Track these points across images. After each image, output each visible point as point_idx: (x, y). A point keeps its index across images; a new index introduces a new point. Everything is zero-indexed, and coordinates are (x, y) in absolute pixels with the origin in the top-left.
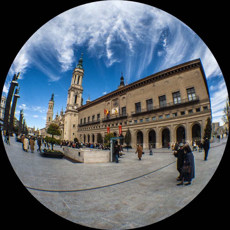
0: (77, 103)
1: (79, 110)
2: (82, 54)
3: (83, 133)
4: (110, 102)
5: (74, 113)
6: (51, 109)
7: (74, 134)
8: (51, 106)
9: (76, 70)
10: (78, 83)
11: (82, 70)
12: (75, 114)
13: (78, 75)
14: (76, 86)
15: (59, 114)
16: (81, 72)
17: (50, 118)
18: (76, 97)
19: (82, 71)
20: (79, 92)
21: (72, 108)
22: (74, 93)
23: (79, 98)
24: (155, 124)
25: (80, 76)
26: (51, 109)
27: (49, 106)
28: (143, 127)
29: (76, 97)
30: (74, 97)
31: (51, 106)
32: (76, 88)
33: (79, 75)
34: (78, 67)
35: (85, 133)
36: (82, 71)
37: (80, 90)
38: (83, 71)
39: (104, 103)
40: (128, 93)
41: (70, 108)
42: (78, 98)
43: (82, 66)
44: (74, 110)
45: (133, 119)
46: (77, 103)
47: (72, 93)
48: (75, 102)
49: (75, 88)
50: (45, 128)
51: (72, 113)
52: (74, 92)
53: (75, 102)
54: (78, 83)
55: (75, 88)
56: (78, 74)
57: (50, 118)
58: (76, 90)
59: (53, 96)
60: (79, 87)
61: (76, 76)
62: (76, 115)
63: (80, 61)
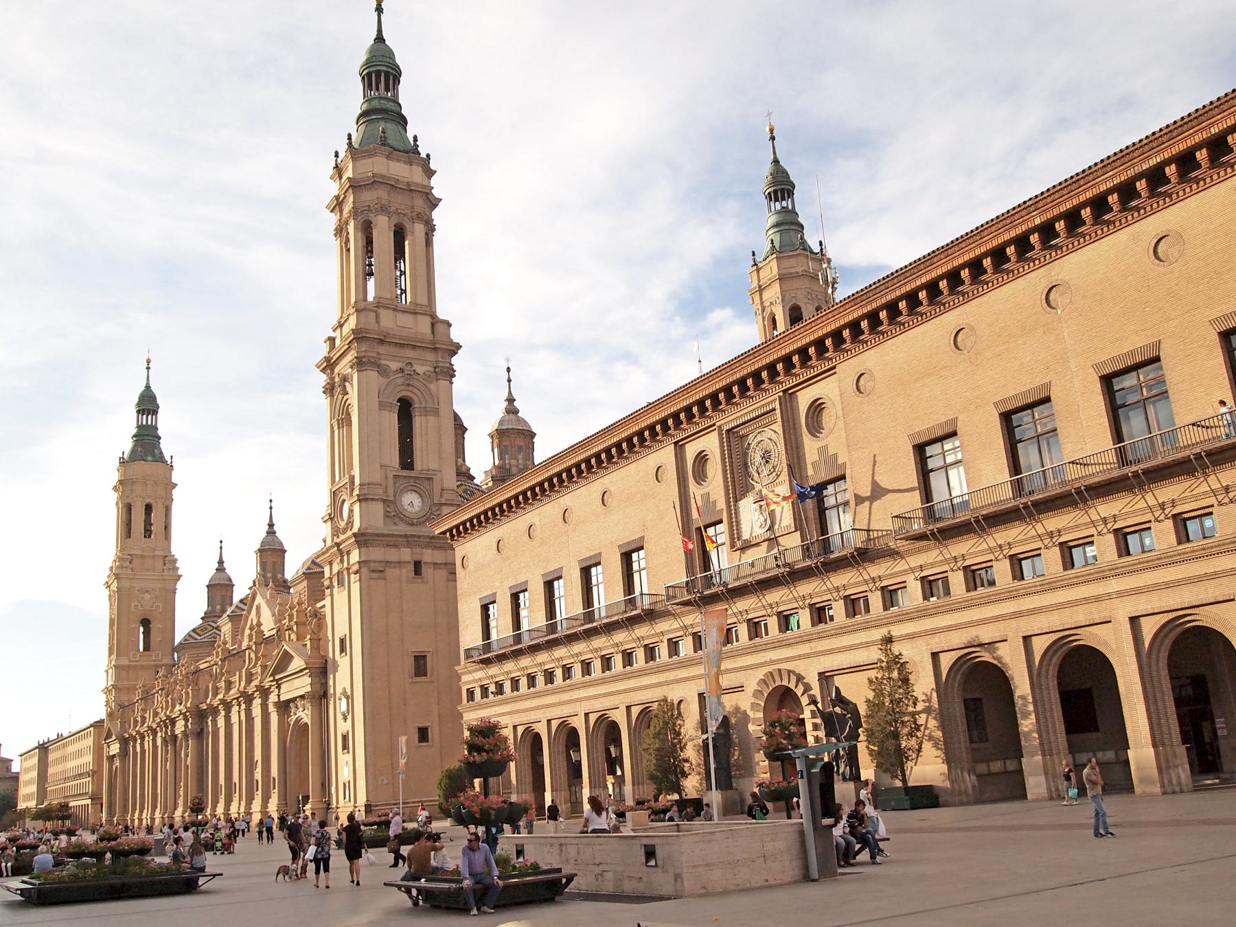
3: (517, 719)
5: (406, 554)
6: (148, 533)
7: (423, 734)
8: (148, 508)
12: (418, 567)
13: (389, 215)
15: (244, 575)
20: (421, 369)
21: (387, 515)
22: (383, 380)
24: (1097, 599)
25: (408, 225)
26: (148, 533)
28: (1002, 624)
30: (391, 420)
31: (148, 508)
33: (395, 220)
35: (532, 716)
39: (664, 455)
40: (848, 368)
42: (418, 422)
44: (403, 529)
45: (912, 570)
46: (418, 464)
50: (98, 725)
51: (392, 554)
52: (383, 371)
55: (382, 342)
56: (383, 209)
58: (395, 358)
62: (427, 571)
63: (378, 73)
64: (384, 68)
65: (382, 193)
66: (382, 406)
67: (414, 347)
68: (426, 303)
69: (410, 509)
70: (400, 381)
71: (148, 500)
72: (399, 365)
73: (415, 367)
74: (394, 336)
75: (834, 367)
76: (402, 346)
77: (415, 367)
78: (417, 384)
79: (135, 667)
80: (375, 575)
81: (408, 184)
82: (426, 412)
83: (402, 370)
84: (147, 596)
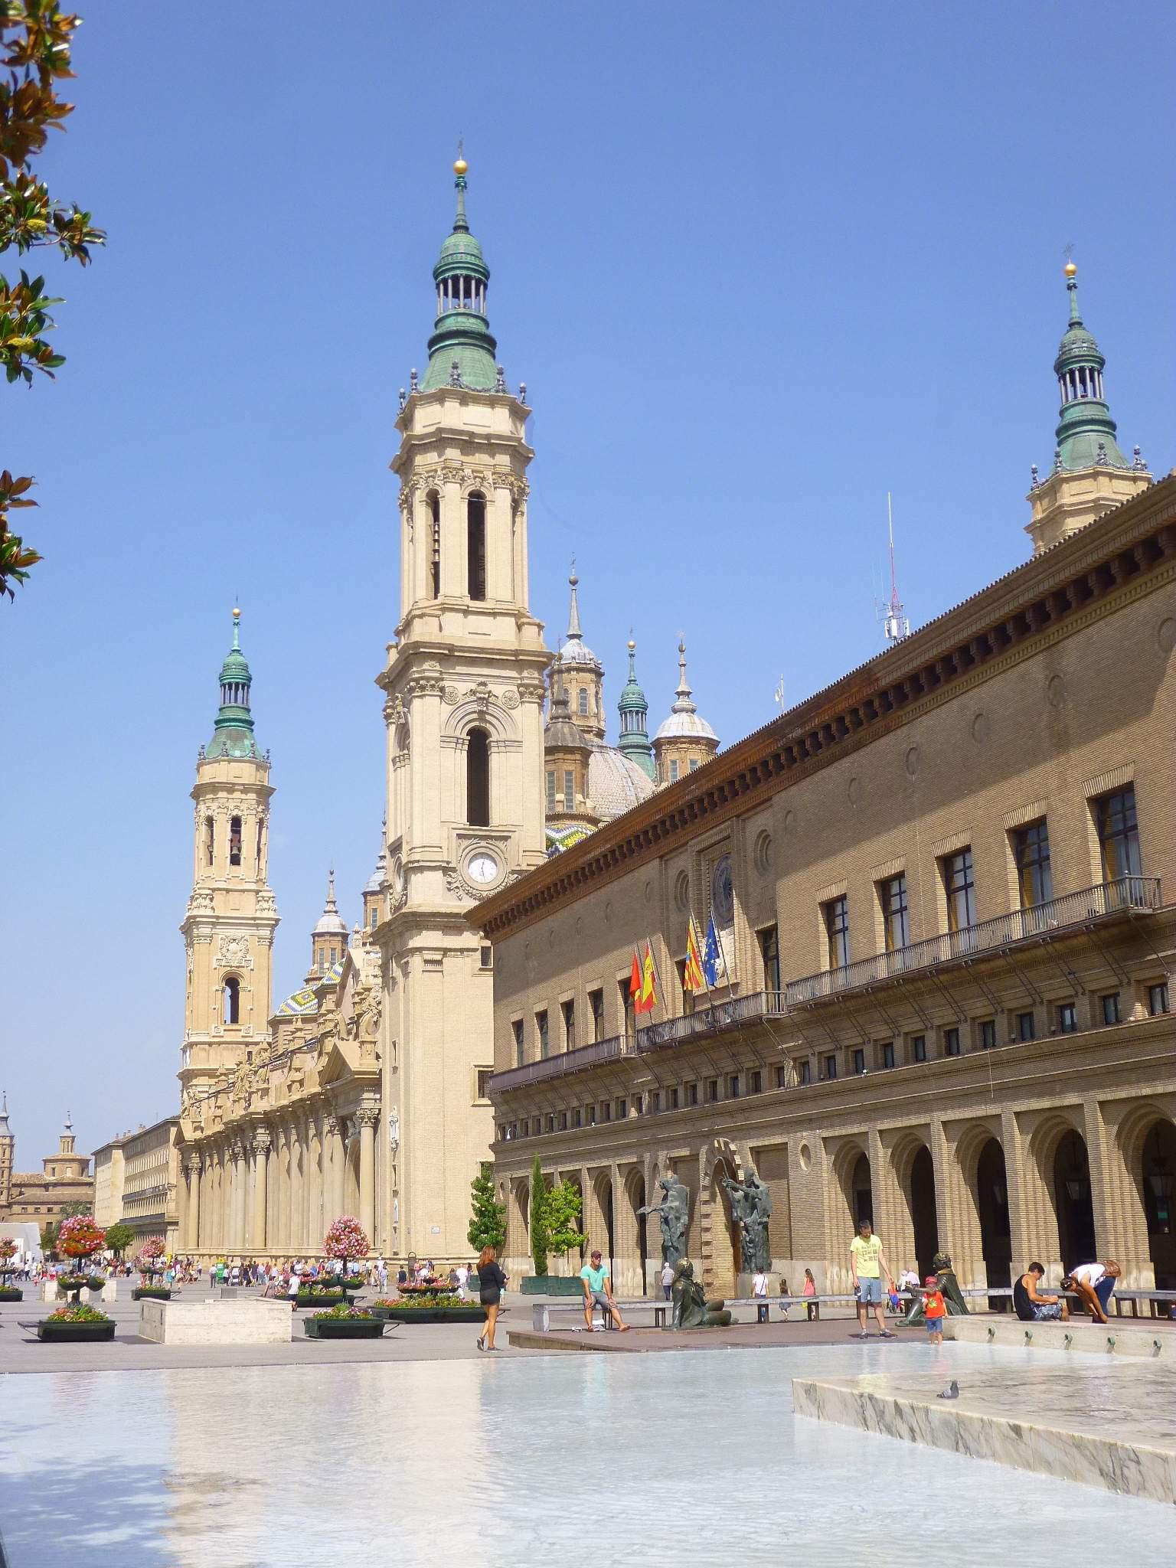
0: (500, 811)
1: (501, 918)
2: (461, 164)
4: (684, 861)
6: (235, 860)
8: (236, 823)
9: (425, 419)
10: (477, 589)
11: (492, 402)
14: (458, 630)
16: (490, 445)
17: (232, 982)
18: (478, 747)
19: (496, 421)
20: (498, 690)
22: (447, 709)
26: (235, 860)
27: (210, 821)
29: (478, 747)
30: (459, 762)
31: (236, 823)
32: (452, 648)
34: (436, 373)
36: (496, 421)
37: (516, 660)
38: (519, 413)
39: (649, 870)
41: (428, 893)
42: (497, 762)
43: (487, 343)
47: (430, 717)
48: (478, 808)
49: (449, 656)
53: (478, 808)
54: (477, 589)
56: (452, 473)
59: (237, 685)
60: (500, 634)
61: (434, 502)
64: (464, 272)
65: (453, 453)
66: (445, 739)
67: (490, 663)
68: (509, 598)
69: (479, 879)
70: (475, 707)
71: (234, 813)
72: (473, 686)
73: (490, 687)
74: (462, 649)
75: (769, 799)
76: (473, 662)
77: (490, 687)
78: (491, 709)
79: (219, 1044)
80: (430, 967)
81: (488, 437)
83: (473, 692)
84: (233, 946)
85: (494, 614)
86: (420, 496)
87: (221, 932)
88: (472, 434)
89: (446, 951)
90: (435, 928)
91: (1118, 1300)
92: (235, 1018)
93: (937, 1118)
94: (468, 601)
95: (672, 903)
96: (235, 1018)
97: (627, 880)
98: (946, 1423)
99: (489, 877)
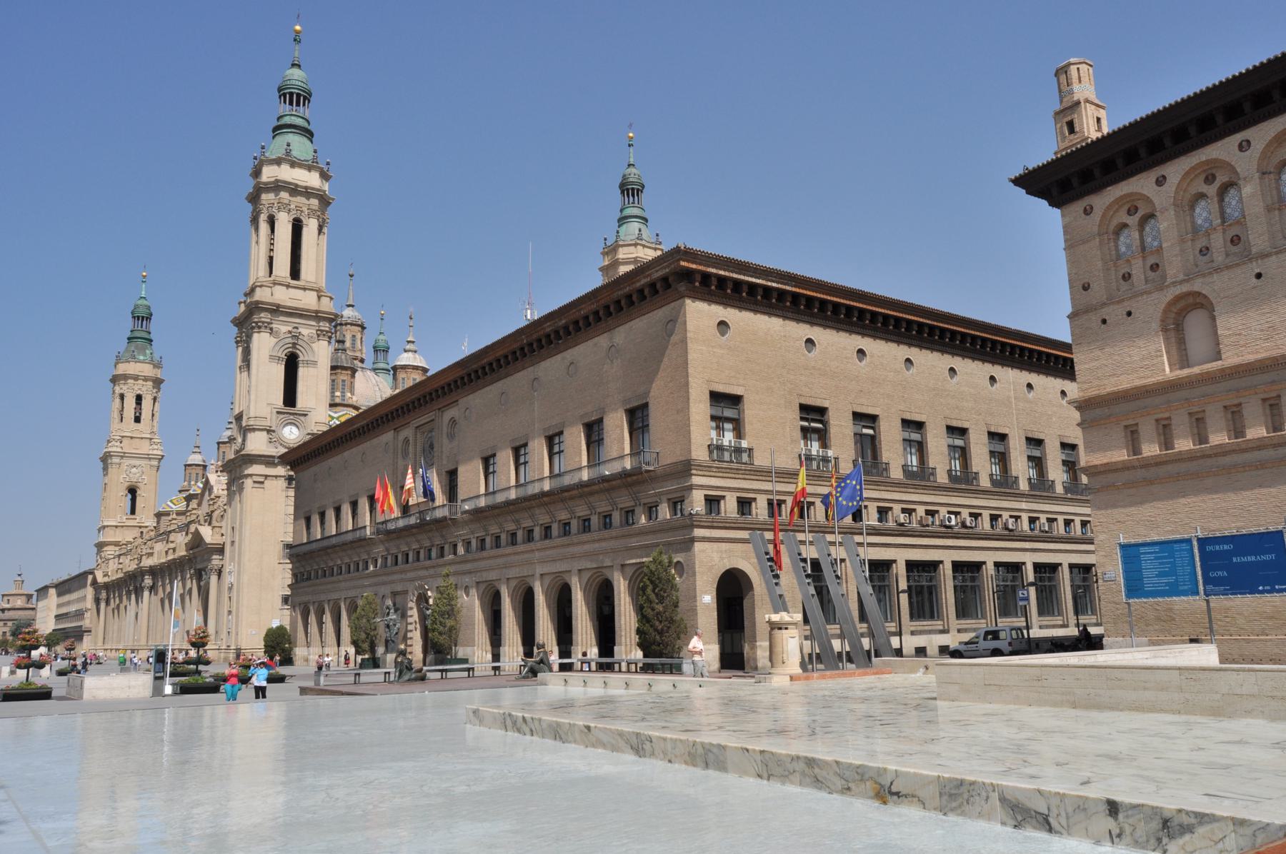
2: (298, 28)
4: (407, 432)
6: (137, 420)
8: (139, 399)
9: (268, 174)
10: (295, 273)
11: (310, 168)
14: (282, 296)
17: (133, 491)
18: (292, 365)
19: (312, 179)
23: (312, 370)
25: (305, 221)
26: (137, 420)
27: (122, 397)
29: (292, 365)
30: (279, 371)
31: (139, 399)
32: (278, 306)
34: (276, 148)
36: (312, 179)
37: (317, 316)
38: (325, 176)
39: (388, 436)
41: (257, 444)
42: (302, 372)
43: (308, 134)
47: (263, 344)
48: (290, 397)
49: (276, 310)
53: (290, 397)
56: (284, 207)
57: (133, 491)
59: (142, 317)
60: (308, 300)
61: (272, 222)
67: (301, 316)
70: (290, 340)
74: (284, 307)
78: (300, 342)
81: (306, 188)
82: (308, 363)
85: (305, 289)
86: (263, 217)
87: (126, 462)
88: (297, 185)
89: (266, 477)
90: (261, 463)
91: (629, 664)
92: (133, 511)
93: (577, 565)
94: (289, 280)
95: (400, 456)
96: (133, 511)
97: (375, 441)
98: (550, 726)
99: (293, 437)
